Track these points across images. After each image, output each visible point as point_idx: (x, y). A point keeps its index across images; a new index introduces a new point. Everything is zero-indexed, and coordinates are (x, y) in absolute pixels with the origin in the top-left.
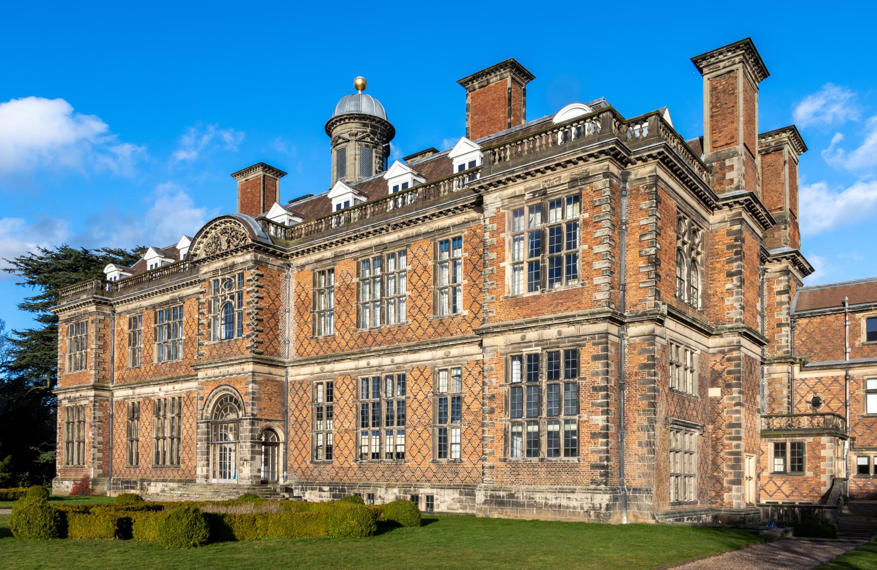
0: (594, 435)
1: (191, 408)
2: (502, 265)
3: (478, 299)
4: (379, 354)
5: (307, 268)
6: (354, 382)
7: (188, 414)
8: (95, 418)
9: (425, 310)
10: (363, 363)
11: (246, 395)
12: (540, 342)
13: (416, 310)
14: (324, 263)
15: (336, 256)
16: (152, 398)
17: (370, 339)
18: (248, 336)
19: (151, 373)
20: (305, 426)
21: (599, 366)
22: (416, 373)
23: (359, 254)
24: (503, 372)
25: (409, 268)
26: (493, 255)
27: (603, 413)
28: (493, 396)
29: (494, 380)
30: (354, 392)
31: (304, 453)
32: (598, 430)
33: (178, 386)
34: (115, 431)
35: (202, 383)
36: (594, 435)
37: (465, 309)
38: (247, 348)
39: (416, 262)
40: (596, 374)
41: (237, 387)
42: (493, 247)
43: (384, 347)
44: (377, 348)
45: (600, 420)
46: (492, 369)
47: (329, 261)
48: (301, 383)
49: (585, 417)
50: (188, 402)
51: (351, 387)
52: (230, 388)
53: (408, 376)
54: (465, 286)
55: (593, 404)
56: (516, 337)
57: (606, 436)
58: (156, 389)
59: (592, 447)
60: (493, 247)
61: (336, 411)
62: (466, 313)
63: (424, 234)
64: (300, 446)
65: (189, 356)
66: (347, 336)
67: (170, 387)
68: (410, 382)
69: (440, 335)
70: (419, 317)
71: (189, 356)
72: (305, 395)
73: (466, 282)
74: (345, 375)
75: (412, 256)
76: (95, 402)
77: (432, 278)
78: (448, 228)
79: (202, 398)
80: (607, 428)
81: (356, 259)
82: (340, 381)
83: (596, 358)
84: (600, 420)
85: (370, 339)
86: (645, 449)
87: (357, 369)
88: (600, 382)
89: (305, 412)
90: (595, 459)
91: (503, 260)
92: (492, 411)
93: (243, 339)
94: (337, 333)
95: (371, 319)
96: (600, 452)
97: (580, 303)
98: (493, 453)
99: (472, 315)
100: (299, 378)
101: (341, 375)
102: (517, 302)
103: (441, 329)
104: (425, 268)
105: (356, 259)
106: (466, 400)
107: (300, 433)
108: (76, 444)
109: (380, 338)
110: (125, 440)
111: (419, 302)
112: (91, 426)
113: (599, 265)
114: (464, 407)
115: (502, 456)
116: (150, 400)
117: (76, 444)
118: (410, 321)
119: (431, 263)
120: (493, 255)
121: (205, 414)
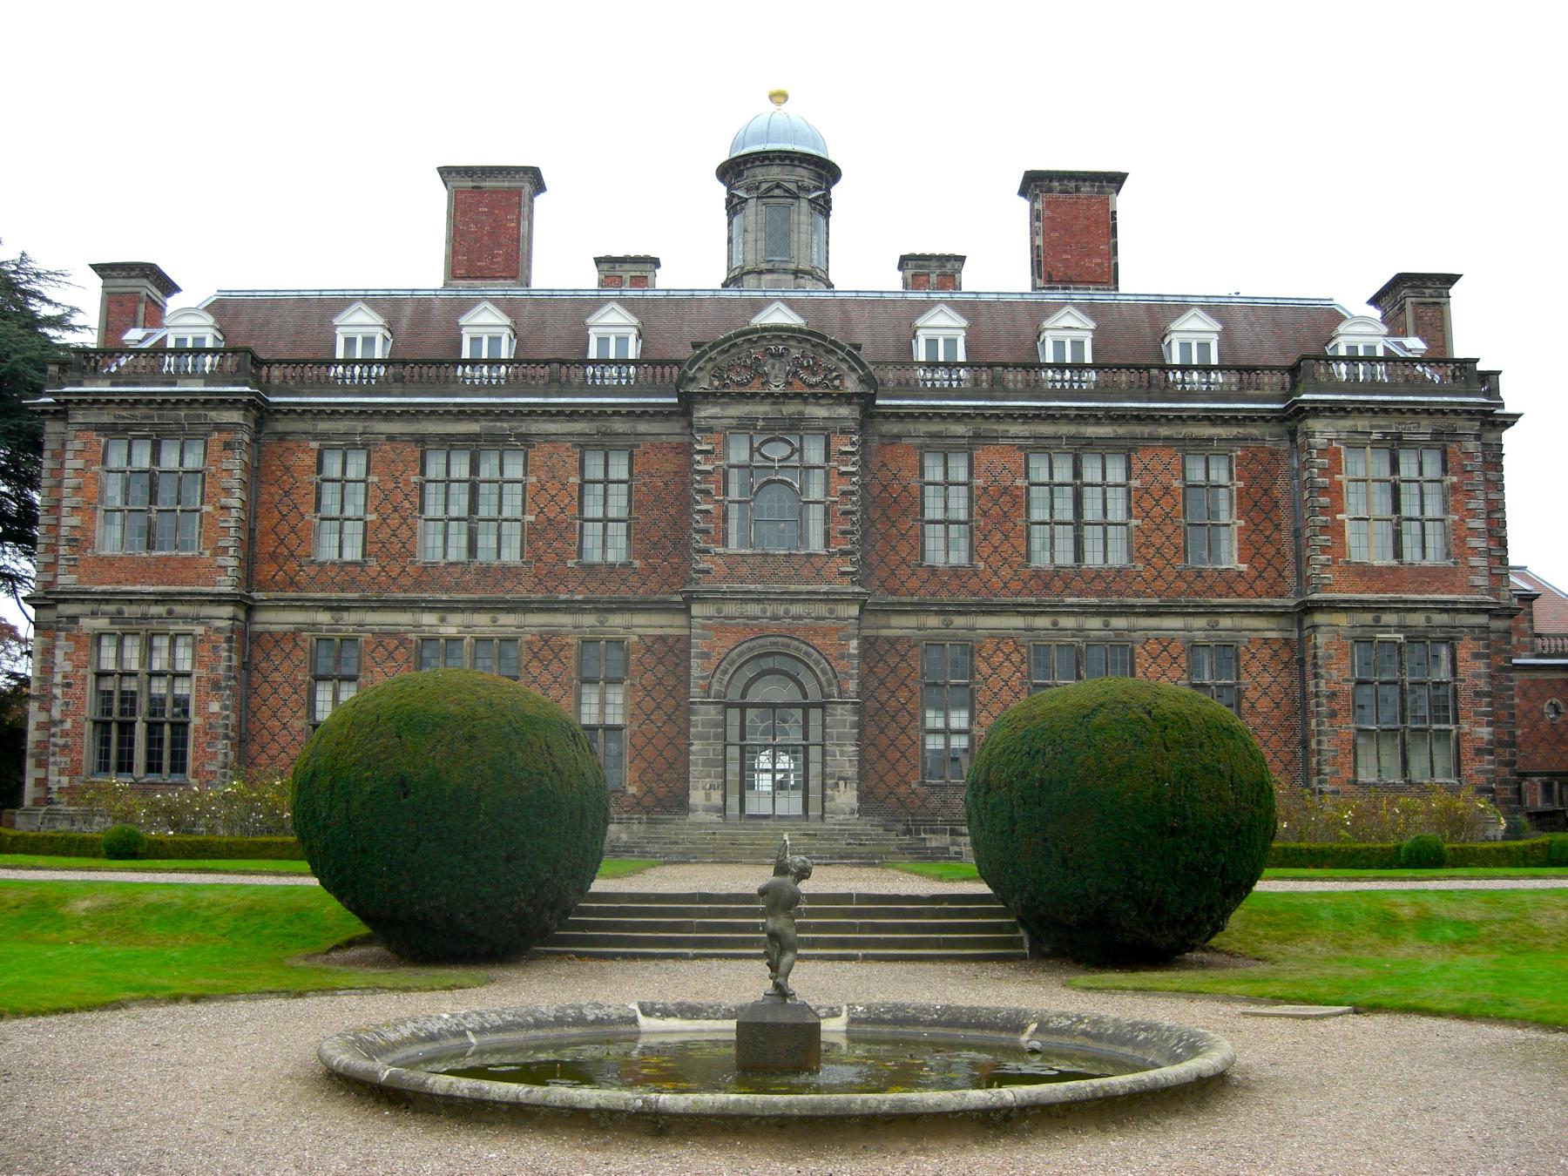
0: (1479, 752)
1: (555, 667)
2: (1339, 517)
3: (1263, 550)
4: (1085, 611)
5: (904, 441)
6: (1024, 650)
7: (546, 678)
8: (230, 668)
9: (1168, 552)
10: (1043, 622)
11: (843, 657)
12: (1400, 628)
13: (1152, 551)
14: (948, 441)
15: (977, 436)
16: (411, 636)
17: (1058, 583)
18: (844, 553)
19: (407, 582)
20: (904, 719)
21: (1481, 666)
22: (1153, 647)
23: (1031, 442)
24: (1348, 662)
25: (1135, 483)
26: (1324, 500)
27: (1489, 724)
28: (1334, 694)
29: (1335, 673)
30: (1024, 667)
31: (902, 767)
32: (1483, 746)
33: (505, 619)
34: (256, 701)
35: (704, 627)
36: (1479, 752)
37: (1241, 561)
38: (844, 574)
39: (1148, 478)
40: (1478, 676)
41: (817, 642)
42: (1324, 490)
43: (1094, 600)
44: (1074, 600)
45: (1485, 732)
46: (1330, 657)
47: (962, 441)
48: (892, 642)
49: (1466, 728)
50: (547, 653)
51: (1015, 657)
52: (796, 643)
53: (1138, 649)
54: (1240, 528)
55: (1477, 714)
56: (1368, 618)
57: (1491, 754)
58: (429, 619)
59: (1476, 766)
60: (1324, 490)
61: (980, 696)
62: (1244, 567)
63: (1166, 438)
64: (893, 755)
65: (550, 558)
66: (1005, 572)
67: (482, 619)
68: (1142, 660)
69: (1197, 594)
70: (1159, 563)
71: (550, 558)
72: (903, 665)
73: (1242, 523)
74: (1000, 638)
75: (1141, 466)
76: (232, 631)
77: (1180, 507)
78: (1211, 439)
79: (706, 656)
80: (1490, 742)
81: (1021, 448)
82: (989, 645)
83: (1477, 656)
84: (1485, 732)
85: (1058, 583)
86: (1507, 770)
87: (1033, 630)
88: (1483, 685)
89: (903, 695)
90: (1481, 780)
91: (1341, 512)
92: (1333, 715)
93: (832, 555)
94: (981, 565)
95: (1051, 551)
96: (1487, 771)
97: (1453, 585)
98: (1337, 772)
99: (1254, 573)
100: (885, 632)
101: (992, 637)
102: (1365, 572)
103: (1198, 586)
104: (1167, 490)
105: (1021, 448)
106: (1248, 694)
107: (892, 731)
108: (140, 730)
109: (1079, 584)
110: (299, 724)
111: (1157, 539)
112: (216, 686)
113: (1475, 542)
114: (1245, 705)
115: (1351, 776)
116: (403, 641)
117: (140, 730)
118: (1140, 566)
119: (1176, 484)
120: (1324, 500)
121: (715, 687)
